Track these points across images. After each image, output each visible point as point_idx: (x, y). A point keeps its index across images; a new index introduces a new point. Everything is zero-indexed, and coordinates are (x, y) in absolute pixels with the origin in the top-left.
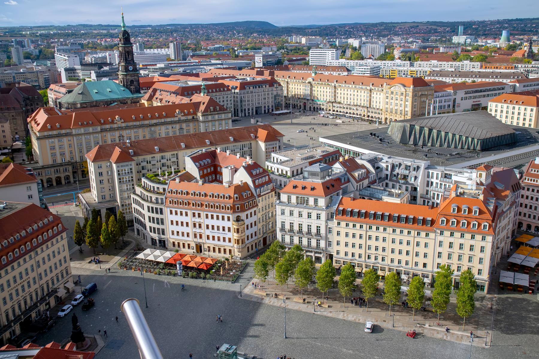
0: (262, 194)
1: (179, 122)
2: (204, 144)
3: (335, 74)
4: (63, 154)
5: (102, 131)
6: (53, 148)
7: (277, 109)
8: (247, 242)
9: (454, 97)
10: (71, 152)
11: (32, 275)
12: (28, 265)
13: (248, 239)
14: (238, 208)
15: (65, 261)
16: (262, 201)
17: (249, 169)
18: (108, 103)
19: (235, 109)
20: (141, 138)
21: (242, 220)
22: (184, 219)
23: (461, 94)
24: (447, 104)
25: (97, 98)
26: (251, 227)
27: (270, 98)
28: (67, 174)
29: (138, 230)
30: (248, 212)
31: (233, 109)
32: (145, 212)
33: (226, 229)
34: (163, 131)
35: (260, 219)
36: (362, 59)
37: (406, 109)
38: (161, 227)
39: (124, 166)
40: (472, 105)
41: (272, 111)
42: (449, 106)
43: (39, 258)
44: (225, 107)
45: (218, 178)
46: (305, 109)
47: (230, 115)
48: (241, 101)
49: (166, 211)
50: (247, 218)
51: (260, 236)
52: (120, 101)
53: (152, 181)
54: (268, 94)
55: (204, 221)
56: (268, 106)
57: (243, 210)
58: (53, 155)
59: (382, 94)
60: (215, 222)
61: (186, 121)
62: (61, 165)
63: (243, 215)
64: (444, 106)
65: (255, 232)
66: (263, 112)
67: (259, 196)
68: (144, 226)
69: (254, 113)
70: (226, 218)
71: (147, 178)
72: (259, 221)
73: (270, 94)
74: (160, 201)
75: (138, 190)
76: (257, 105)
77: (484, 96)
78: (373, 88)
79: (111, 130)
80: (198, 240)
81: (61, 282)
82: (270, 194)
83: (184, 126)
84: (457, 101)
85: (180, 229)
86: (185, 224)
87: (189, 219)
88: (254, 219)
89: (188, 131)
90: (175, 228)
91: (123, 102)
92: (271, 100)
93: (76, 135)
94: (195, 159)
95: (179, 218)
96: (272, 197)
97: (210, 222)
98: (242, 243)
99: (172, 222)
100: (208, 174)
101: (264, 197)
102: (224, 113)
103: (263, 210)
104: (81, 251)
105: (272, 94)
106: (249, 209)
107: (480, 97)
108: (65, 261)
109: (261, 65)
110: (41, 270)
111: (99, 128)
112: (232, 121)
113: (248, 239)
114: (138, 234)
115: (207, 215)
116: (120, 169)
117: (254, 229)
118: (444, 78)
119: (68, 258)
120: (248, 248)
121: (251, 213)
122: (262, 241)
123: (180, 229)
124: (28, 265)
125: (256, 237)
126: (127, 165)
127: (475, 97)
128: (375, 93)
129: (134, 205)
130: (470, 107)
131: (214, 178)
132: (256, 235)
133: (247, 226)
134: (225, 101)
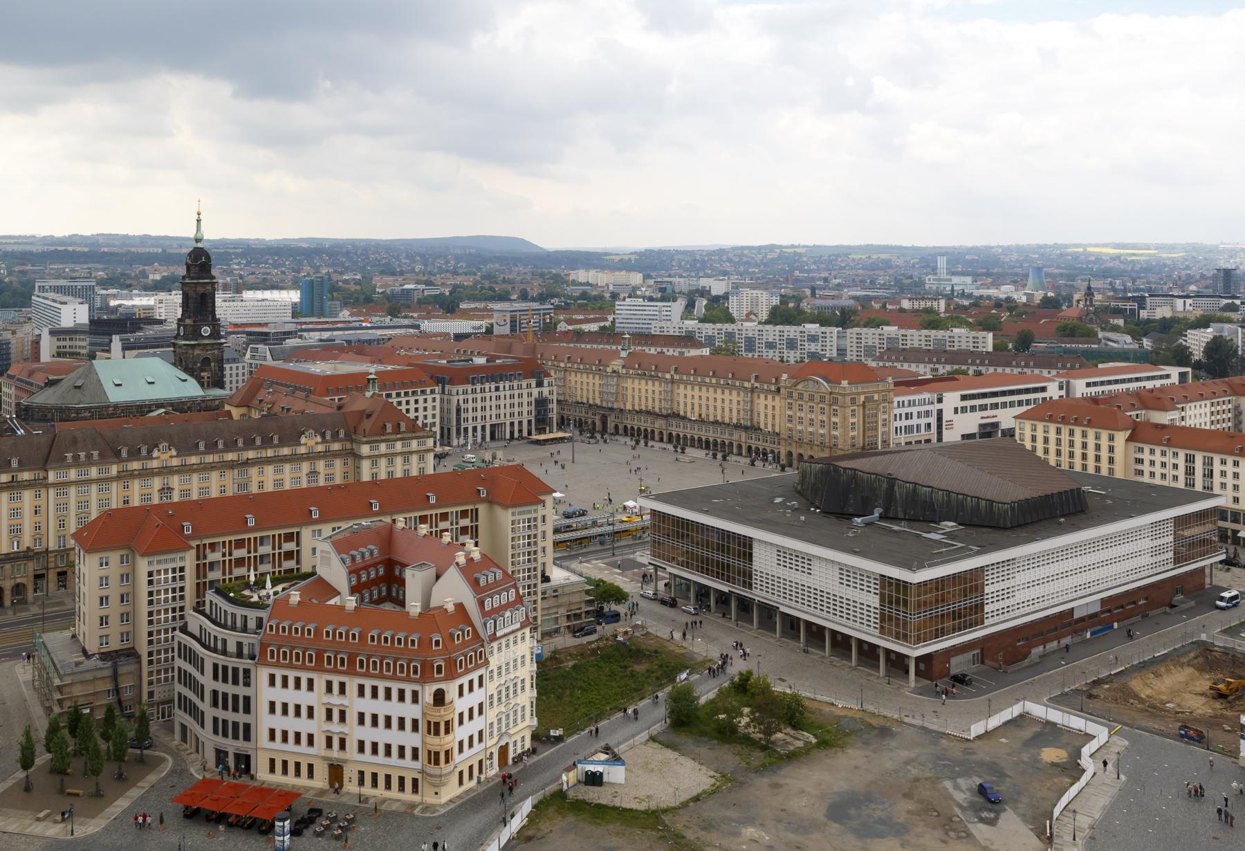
0: (498, 634)
1: (311, 457)
2: (368, 512)
3: (670, 352)
7: (541, 430)
8: (457, 758)
9: (939, 406)
10: (38, 528)
13: (461, 751)
14: (439, 668)
16: (499, 649)
17: (470, 571)
18: (140, 409)
19: (442, 428)
20: (214, 494)
22: (303, 698)
23: (952, 399)
26: (471, 717)
27: (525, 404)
28: (19, 581)
29: (184, 728)
30: (464, 681)
31: (437, 429)
32: (207, 681)
33: (408, 724)
35: (491, 696)
36: (732, 321)
37: (833, 433)
38: (241, 718)
39: (166, 561)
40: (981, 425)
41: (530, 433)
42: (929, 425)
44: (419, 423)
45: (394, 594)
46: (604, 430)
47: (430, 442)
48: (458, 411)
49: (262, 675)
50: (461, 694)
51: (492, 744)
52: (172, 405)
53: (230, 600)
54: (520, 396)
56: (520, 423)
57: (451, 676)
59: (777, 398)
60: (381, 707)
61: (328, 455)
63: (451, 689)
64: (918, 426)
65: (481, 733)
66: (508, 436)
67: (494, 638)
68: (199, 717)
69: (488, 439)
70: (408, 696)
72: (491, 703)
73: (525, 396)
74: (246, 650)
75: (196, 622)
76: (494, 421)
77: (1004, 405)
78: (757, 385)
80: (335, 753)
82: (519, 634)
83: (321, 465)
84: (945, 418)
85: (291, 724)
86: (304, 712)
87: (317, 698)
88: (477, 696)
89: (329, 477)
90: (280, 722)
91: (180, 406)
92: (525, 409)
93: (54, 485)
94: (342, 546)
95: (291, 696)
96: (523, 638)
97: (368, 706)
98: (447, 761)
99: (272, 704)
101: (503, 641)
102: (416, 438)
103: (499, 673)
104: (28, 787)
105: (530, 395)
106: (468, 671)
107: (995, 406)
109: (506, 330)
111: (114, 470)
112: (436, 456)
113: (461, 751)
114: (184, 739)
115: (361, 689)
118: (914, 365)
121: (471, 682)
123: (291, 724)
125: (483, 745)
126: (173, 560)
127: (983, 408)
128: (762, 396)
129: (179, 663)
131: (384, 594)
132: (480, 740)
134: (421, 410)
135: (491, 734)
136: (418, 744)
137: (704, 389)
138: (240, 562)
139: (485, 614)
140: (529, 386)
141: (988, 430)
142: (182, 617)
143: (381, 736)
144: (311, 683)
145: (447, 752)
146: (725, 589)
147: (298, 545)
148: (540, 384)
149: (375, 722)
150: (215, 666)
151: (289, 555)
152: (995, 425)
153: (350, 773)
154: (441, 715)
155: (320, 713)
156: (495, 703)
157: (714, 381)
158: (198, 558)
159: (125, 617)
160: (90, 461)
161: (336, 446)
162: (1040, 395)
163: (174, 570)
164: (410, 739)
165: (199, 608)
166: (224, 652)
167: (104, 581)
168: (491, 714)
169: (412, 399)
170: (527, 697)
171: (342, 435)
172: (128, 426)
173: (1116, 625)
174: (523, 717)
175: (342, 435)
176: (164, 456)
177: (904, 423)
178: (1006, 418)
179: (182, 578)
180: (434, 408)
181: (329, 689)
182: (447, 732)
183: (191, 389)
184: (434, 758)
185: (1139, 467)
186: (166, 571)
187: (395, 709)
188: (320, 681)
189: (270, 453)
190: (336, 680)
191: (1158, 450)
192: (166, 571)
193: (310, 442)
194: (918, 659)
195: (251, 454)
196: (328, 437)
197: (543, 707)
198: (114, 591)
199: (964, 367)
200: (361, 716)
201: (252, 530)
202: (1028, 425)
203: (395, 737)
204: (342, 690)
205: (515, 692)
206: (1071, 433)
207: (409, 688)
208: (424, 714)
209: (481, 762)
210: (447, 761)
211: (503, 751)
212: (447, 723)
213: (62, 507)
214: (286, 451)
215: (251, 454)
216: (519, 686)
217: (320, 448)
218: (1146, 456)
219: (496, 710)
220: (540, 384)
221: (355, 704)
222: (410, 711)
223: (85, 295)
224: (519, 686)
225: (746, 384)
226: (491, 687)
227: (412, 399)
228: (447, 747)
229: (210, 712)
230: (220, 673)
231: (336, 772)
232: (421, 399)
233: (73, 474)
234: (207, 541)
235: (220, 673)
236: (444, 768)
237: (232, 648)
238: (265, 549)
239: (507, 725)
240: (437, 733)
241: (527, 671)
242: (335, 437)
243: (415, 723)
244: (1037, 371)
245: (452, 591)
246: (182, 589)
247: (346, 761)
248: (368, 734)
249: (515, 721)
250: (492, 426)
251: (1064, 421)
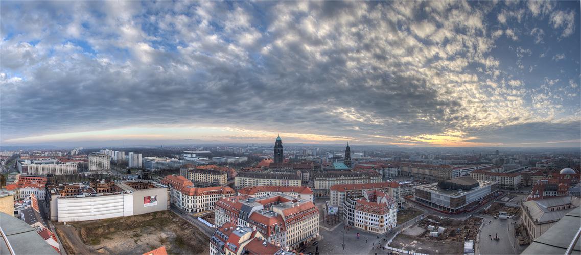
1: (363, 179)
4: (323, 186)
5: (337, 180)
6: (320, 184)
8: (384, 227)
11: (306, 227)
12: (305, 223)
22: (361, 215)
25: (336, 168)
32: (348, 211)
34: (357, 182)
38: (352, 217)
43: (309, 221)
49: (355, 211)
58: (320, 186)
60: (373, 218)
61: (366, 179)
62: (322, 190)
67: (390, 208)
75: (346, 202)
79: (340, 180)
80: (366, 224)
87: (363, 216)
91: (345, 170)
95: (360, 215)
97: (371, 217)
100: (372, 199)
110: (309, 226)
115: (370, 215)
124: (305, 223)
139: (389, 205)
143: (373, 222)
153: (368, 227)
159: (337, 200)
165: (347, 200)
168: (390, 220)
172: (338, 173)
176: (343, 177)
183: (347, 168)
184: (381, 226)
187: (375, 218)
188: (364, 213)
190: (366, 213)
198: (335, 196)
211: (391, 226)
213: (329, 184)
221: (369, 217)
223: (333, 153)
226: (390, 216)
229: (348, 216)
230: (350, 210)
231: (366, 227)
233: (330, 179)
245: (384, 200)
248: (371, 222)
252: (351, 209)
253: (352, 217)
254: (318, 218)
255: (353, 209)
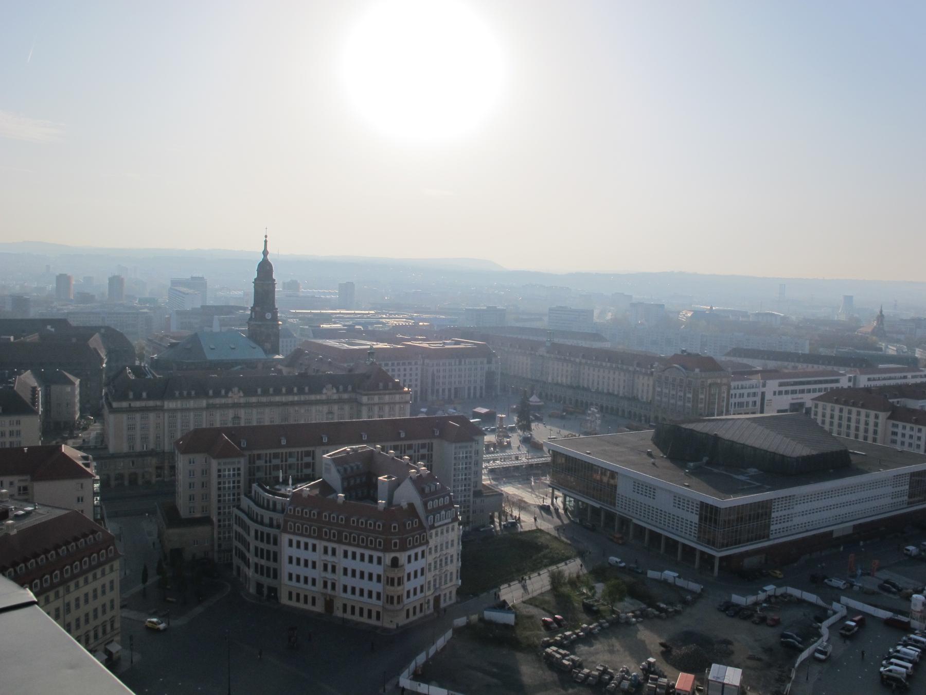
1: (328, 402)
8: (406, 601)
13: (408, 596)
15: (112, 607)
21: (402, 566)
23: (773, 385)
24: (751, 399)
32: (251, 539)
33: (375, 578)
35: (430, 564)
38: (272, 564)
42: (755, 402)
43: (71, 598)
49: (285, 538)
50: (409, 561)
51: (429, 594)
55: (343, 563)
60: (358, 565)
61: (340, 401)
63: (403, 557)
64: (748, 403)
65: (422, 587)
70: (375, 560)
71: (260, 485)
74: (275, 523)
75: (246, 502)
77: (809, 391)
81: (100, 641)
83: (335, 408)
84: (767, 397)
86: (310, 564)
88: (421, 563)
95: (303, 554)
97: (350, 564)
98: (398, 602)
107: (802, 391)
108: (112, 607)
113: (408, 596)
116: (222, 467)
117: (420, 581)
119: (117, 604)
120: (408, 611)
121: (416, 555)
122: (432, 602)
123: (302, 571)
125: (423, 595)
126: (234, 463)
127: (794, 392)
128: (641, 377)
129: (236, 527)
130: (787, 407)
132: (422, 591)
133: (409, 575)
135: (429, 588)
136: (381, 590)
137: (602, 370)
138: (277, 468)
140: (482, 363)
141: (796, 407)
142: (239, 500)
143: (358, 583)
144: (314, 547)
145: (399, 597)
146: (598, 506)
147: (313, 459)
148: (489, 362)
149: (354, 574)
150: (256, 532)
151: (307, 465)
152: (801, 405)
154: (395, 574)
155: (320, 566)
156: (432, 569)
157: (609, 364)
158: (250, 463)
160: (189, 396)
161: (345, 396)
162: (834, 385)
163: (234, 470)
164: (376, 587)
165: (248, 494)
166: (262, 523)
167: (191, 473)
168: (430, 576)
169: (402, 368)
170: (454, 567)
171: (350, 388)
173: (861, 543)
174: (451, 580)
175: (350, 388)
177: (738, 400)
178: (807, 399)
179: (239, 475)
180: (417, 375)
181: (326, 551)
182: (399, 584)
184: (390, 599)
185: (895, 438)
186: (229, 470)
187: (366, 567)
188: (320, 545)
189: (303, 398)
190: (330, 545)
191: (908, 426)
192: (229, 470)
193: (329, 392)
194: (721, 559)
195: (290, 398)
196: (341, 388)
197: (464, 573)
199: (786, 363)
200: (345, 570)
201: (283, 447)
202: (821, 404)
203: (366, 585)
204: (334, 553)
205: (446, 563)
206: (850, 412)
207: (376, 554)
208: (385, 571)
209: (421, 605)
210: (398, 602)
211: (437, 600)
212: (399, 579)
214: (313, 397)
215: (290, 398)
216: (449, 559)
217: (335, 397)
218: (900, 430)
219: (433, 573)
220: (489, 362)
222: (376, 569)
224: (449, 559)
225: (631, 368)
226: (430, 559)
227: (402, 368)
228: (399, 593)
229: (253, 559)
230: (259, 536)
232: (408, 368)
234: (256, 452)
235: (259, 536)
236: (397, 607)
237: (266, 521)
238: (292, 461)
239: (440, 584)
240: (392, 584)
241: (455, 550)
242: (345, 391)
243: (379, 577)
244: (835, 368)
246: (239, 482)
247: (335, 597)
248: (349, 581)
249: (446, 581)
250: (455, 388)
251: (846, 403)
252: (267, 530)
253: (272, 564)
254: (115, 576)
255: (273, 531)
